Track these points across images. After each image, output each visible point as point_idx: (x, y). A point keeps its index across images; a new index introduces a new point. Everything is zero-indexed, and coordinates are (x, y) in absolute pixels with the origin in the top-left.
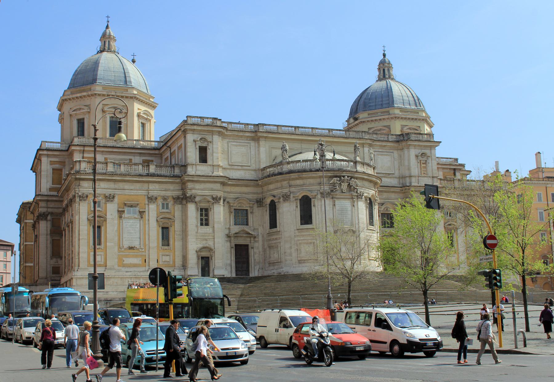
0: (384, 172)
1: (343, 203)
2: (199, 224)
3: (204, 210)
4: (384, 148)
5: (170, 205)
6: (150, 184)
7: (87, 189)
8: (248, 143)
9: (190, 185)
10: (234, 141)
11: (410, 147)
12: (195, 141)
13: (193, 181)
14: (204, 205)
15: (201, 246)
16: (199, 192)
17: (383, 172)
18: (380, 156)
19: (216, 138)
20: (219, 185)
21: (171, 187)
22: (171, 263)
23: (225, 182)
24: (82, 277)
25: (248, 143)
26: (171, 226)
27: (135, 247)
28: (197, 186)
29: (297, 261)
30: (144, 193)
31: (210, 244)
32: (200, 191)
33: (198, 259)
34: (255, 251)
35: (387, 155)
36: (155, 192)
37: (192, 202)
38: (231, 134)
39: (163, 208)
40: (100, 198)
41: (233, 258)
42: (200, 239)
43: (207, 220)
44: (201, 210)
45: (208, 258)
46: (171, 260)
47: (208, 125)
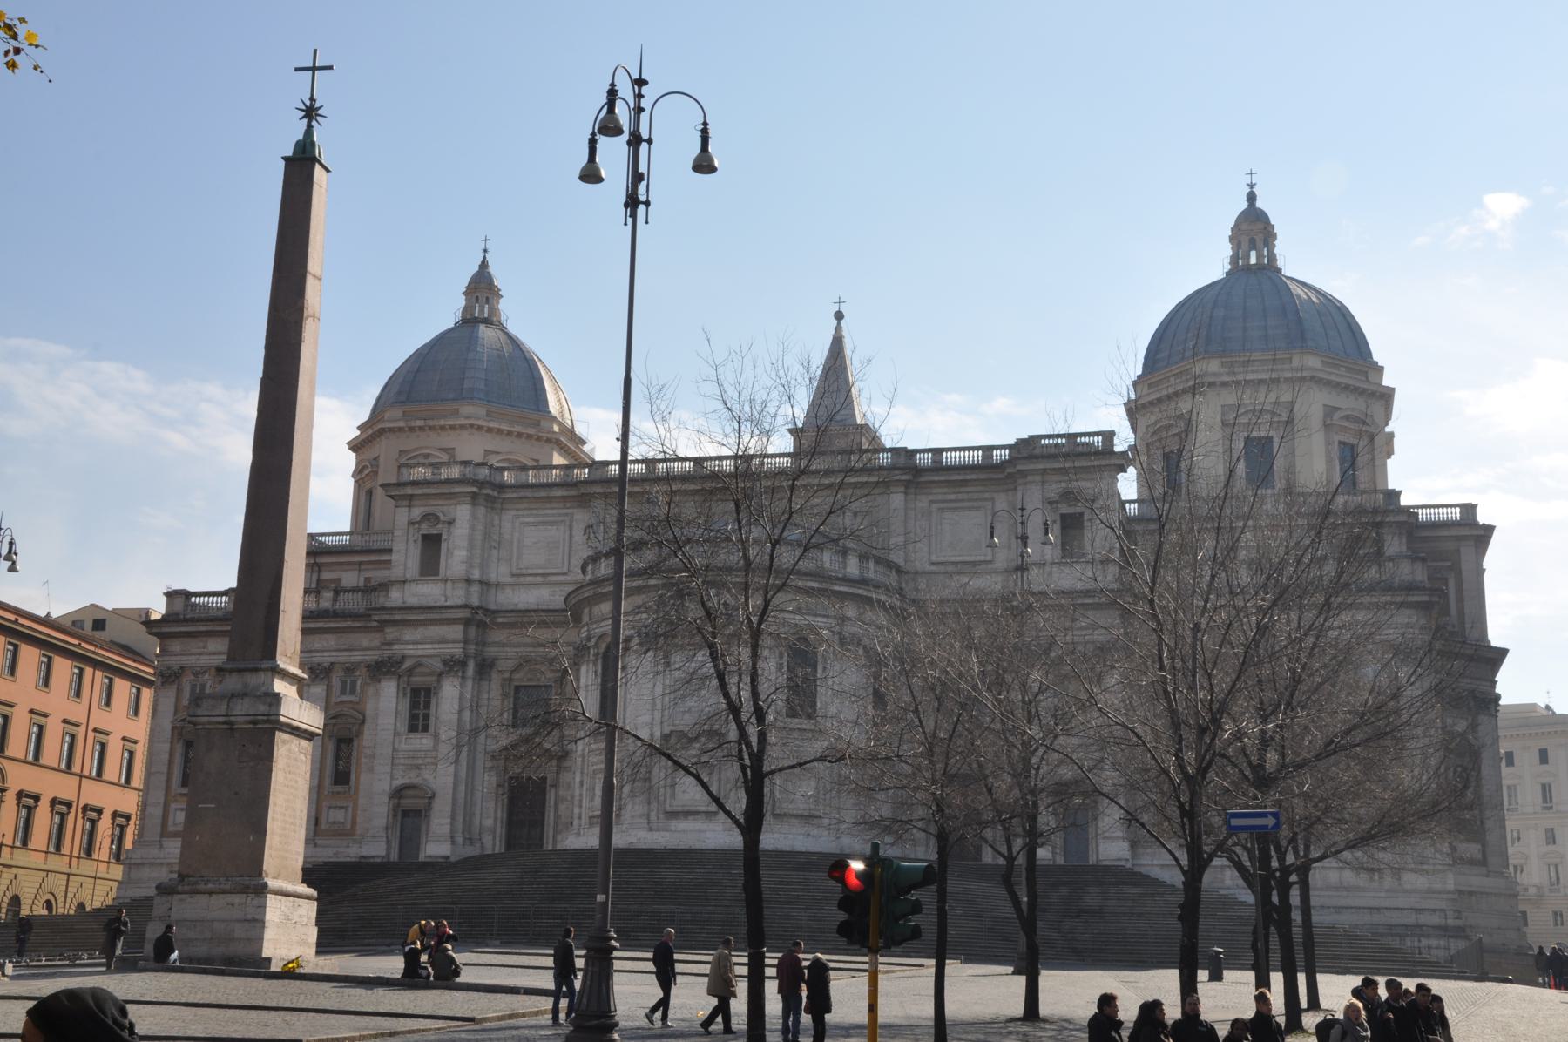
0: (958, 559)
2: (403, 728)
3: (423, 693)
4: (962, 489)
5: (359, 683)
6: (317, 637)
7: (179, 658)
8: (566, 514)
9: (391, 633)
10: (529, 512)
11: (1030, 478)
12: (413, 523)
13: (395, 623)
14: (417, 680)
15: (398, 782)
16: (409, 649)
17: (953, 559)
18: (947, 515)
19: (463, 513)
20: (460, 628)
21: (365, 640)
22: (349, 827)
23: (479, 619)
24: (140, 861)
25: (566, 514)
26: (357, 736)
28: (409, 634)
29: (588, 820)
31: (427, 776)
32: (411, 647)
33: (395, 816)
34: (561, 793)
35: (970, 509)
36: (325, 654)
37: (394, 673)
38: (514, 495)
39: (343, 692)
40: (207, 676)
41: (502, 814)
43: (427, 717)
44: (415, 692)
45: (420, 811)
46: (349, 818)
47: (448, 481)
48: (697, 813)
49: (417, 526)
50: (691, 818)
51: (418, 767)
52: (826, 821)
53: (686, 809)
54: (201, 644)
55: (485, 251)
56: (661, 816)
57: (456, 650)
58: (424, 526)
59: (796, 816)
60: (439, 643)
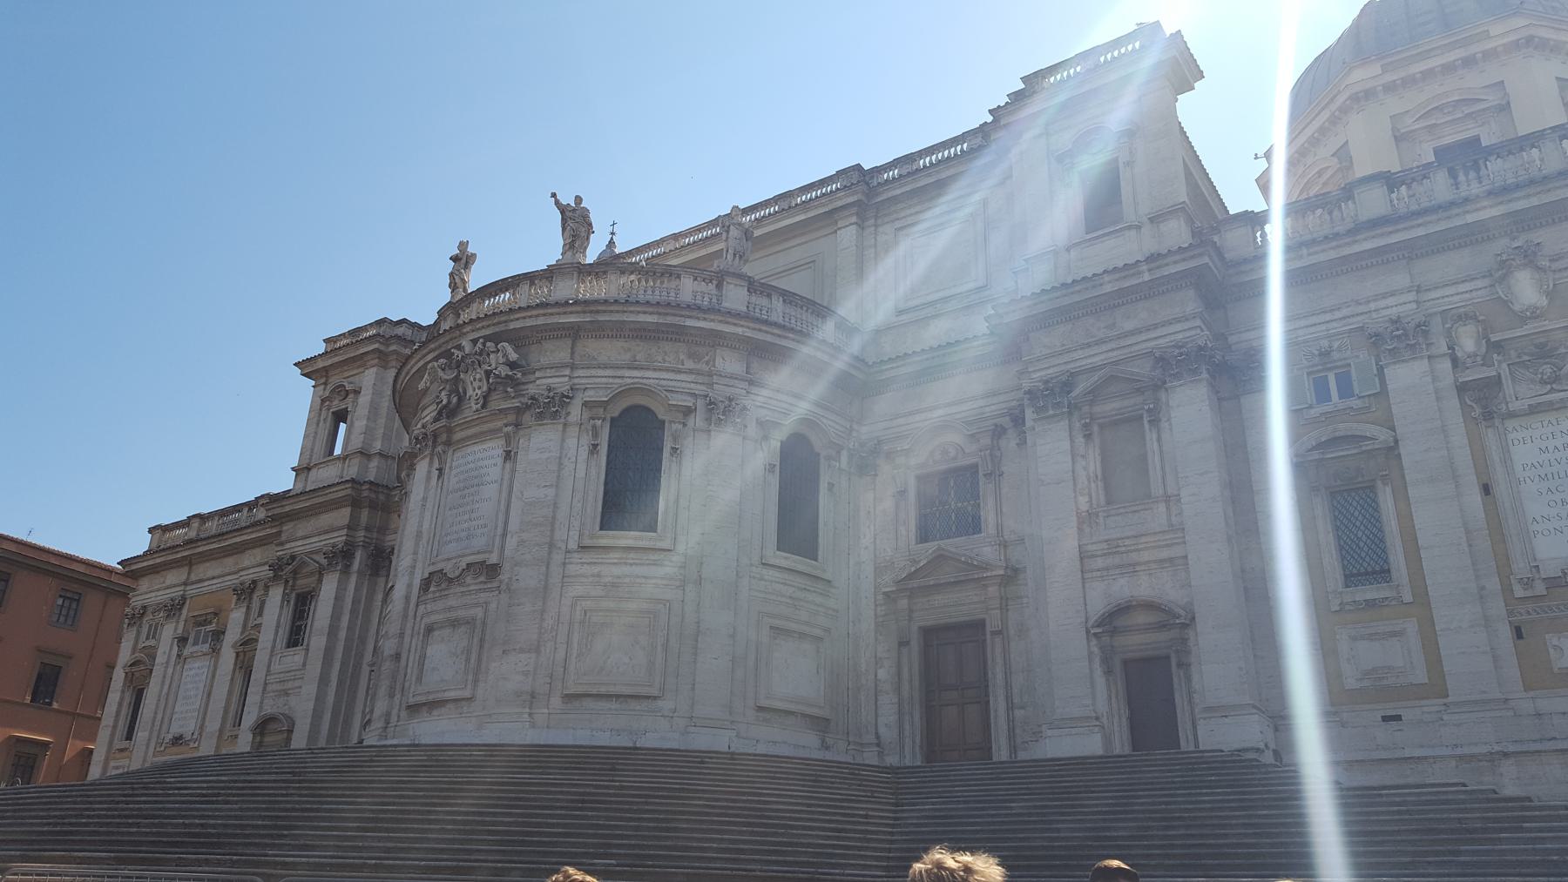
1: (470, 458)
14: (304, 583)
27: (181, 737)
28: (303, 528)
30: (232, 580)
32: (300, 543)
42: (274, 692)
48: (442, 703)
49: (327, 403)
50: (435, 713)
51: (286, 693)
52: (666, 705)
53: (431, 698)
54: (162, 580)
55: (613, 234)
56: (404, 714)
57: (339, 538)
58: (336, 402)
59: (608, 697)
60: (326, 532)
